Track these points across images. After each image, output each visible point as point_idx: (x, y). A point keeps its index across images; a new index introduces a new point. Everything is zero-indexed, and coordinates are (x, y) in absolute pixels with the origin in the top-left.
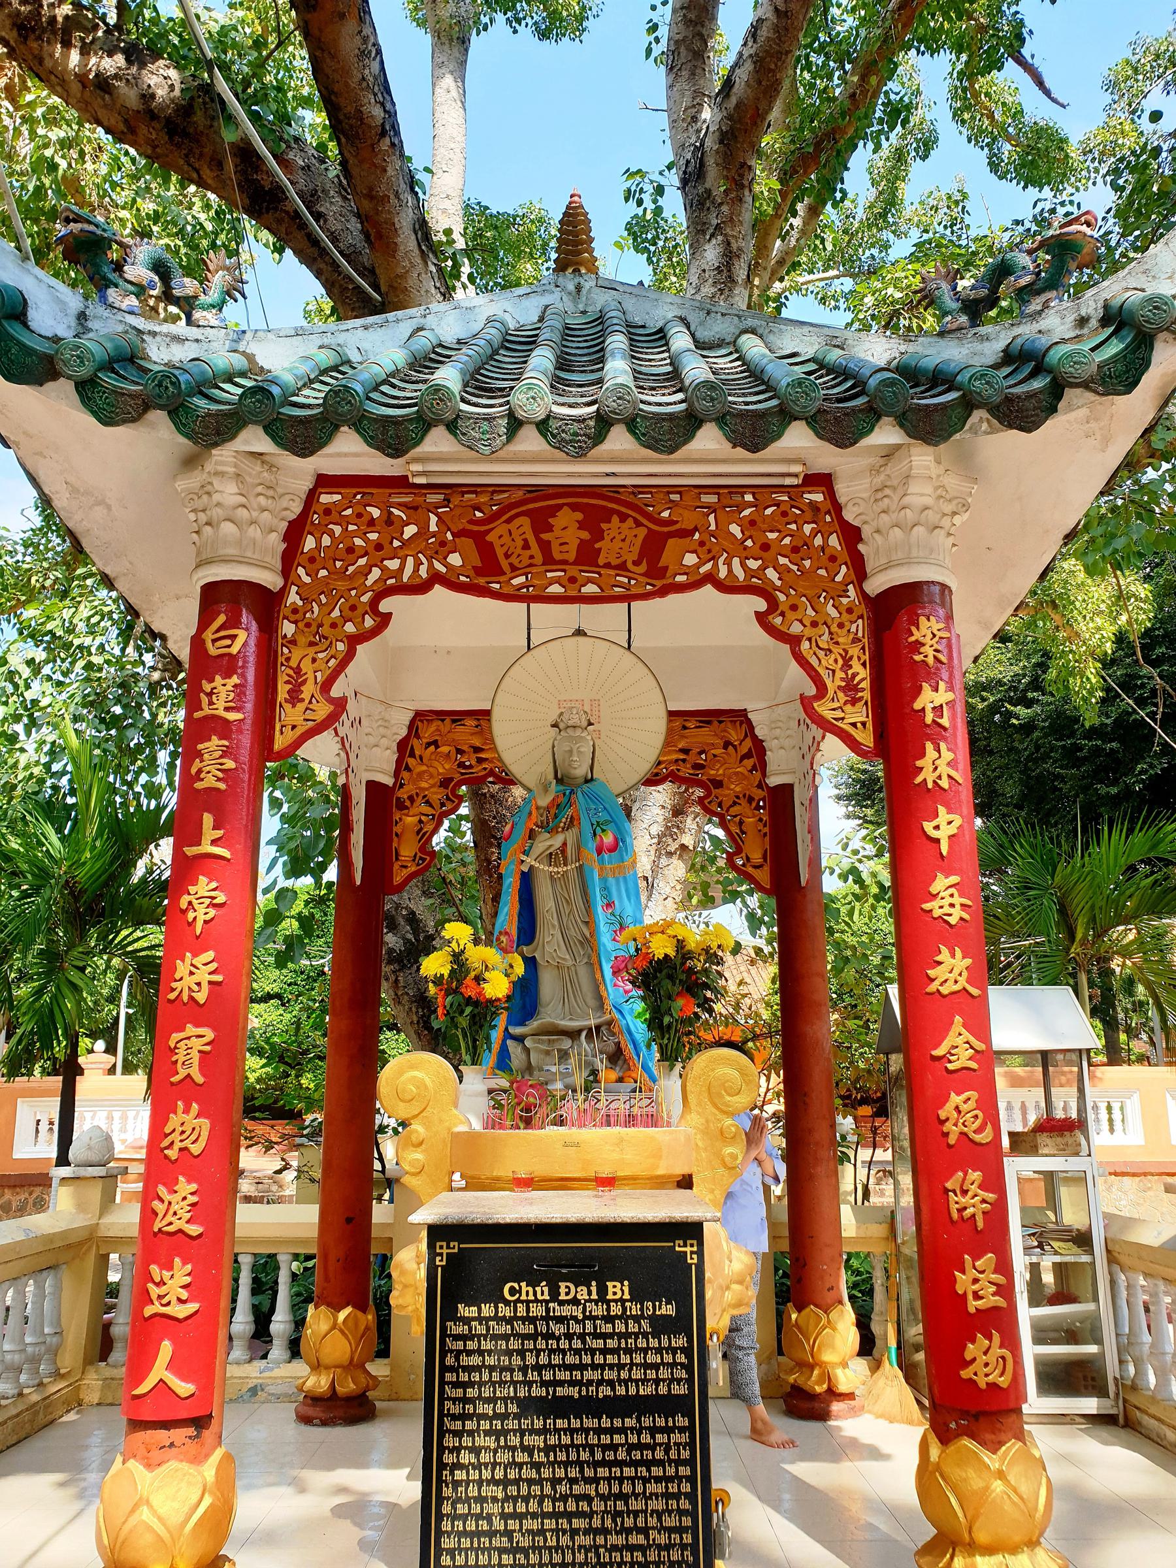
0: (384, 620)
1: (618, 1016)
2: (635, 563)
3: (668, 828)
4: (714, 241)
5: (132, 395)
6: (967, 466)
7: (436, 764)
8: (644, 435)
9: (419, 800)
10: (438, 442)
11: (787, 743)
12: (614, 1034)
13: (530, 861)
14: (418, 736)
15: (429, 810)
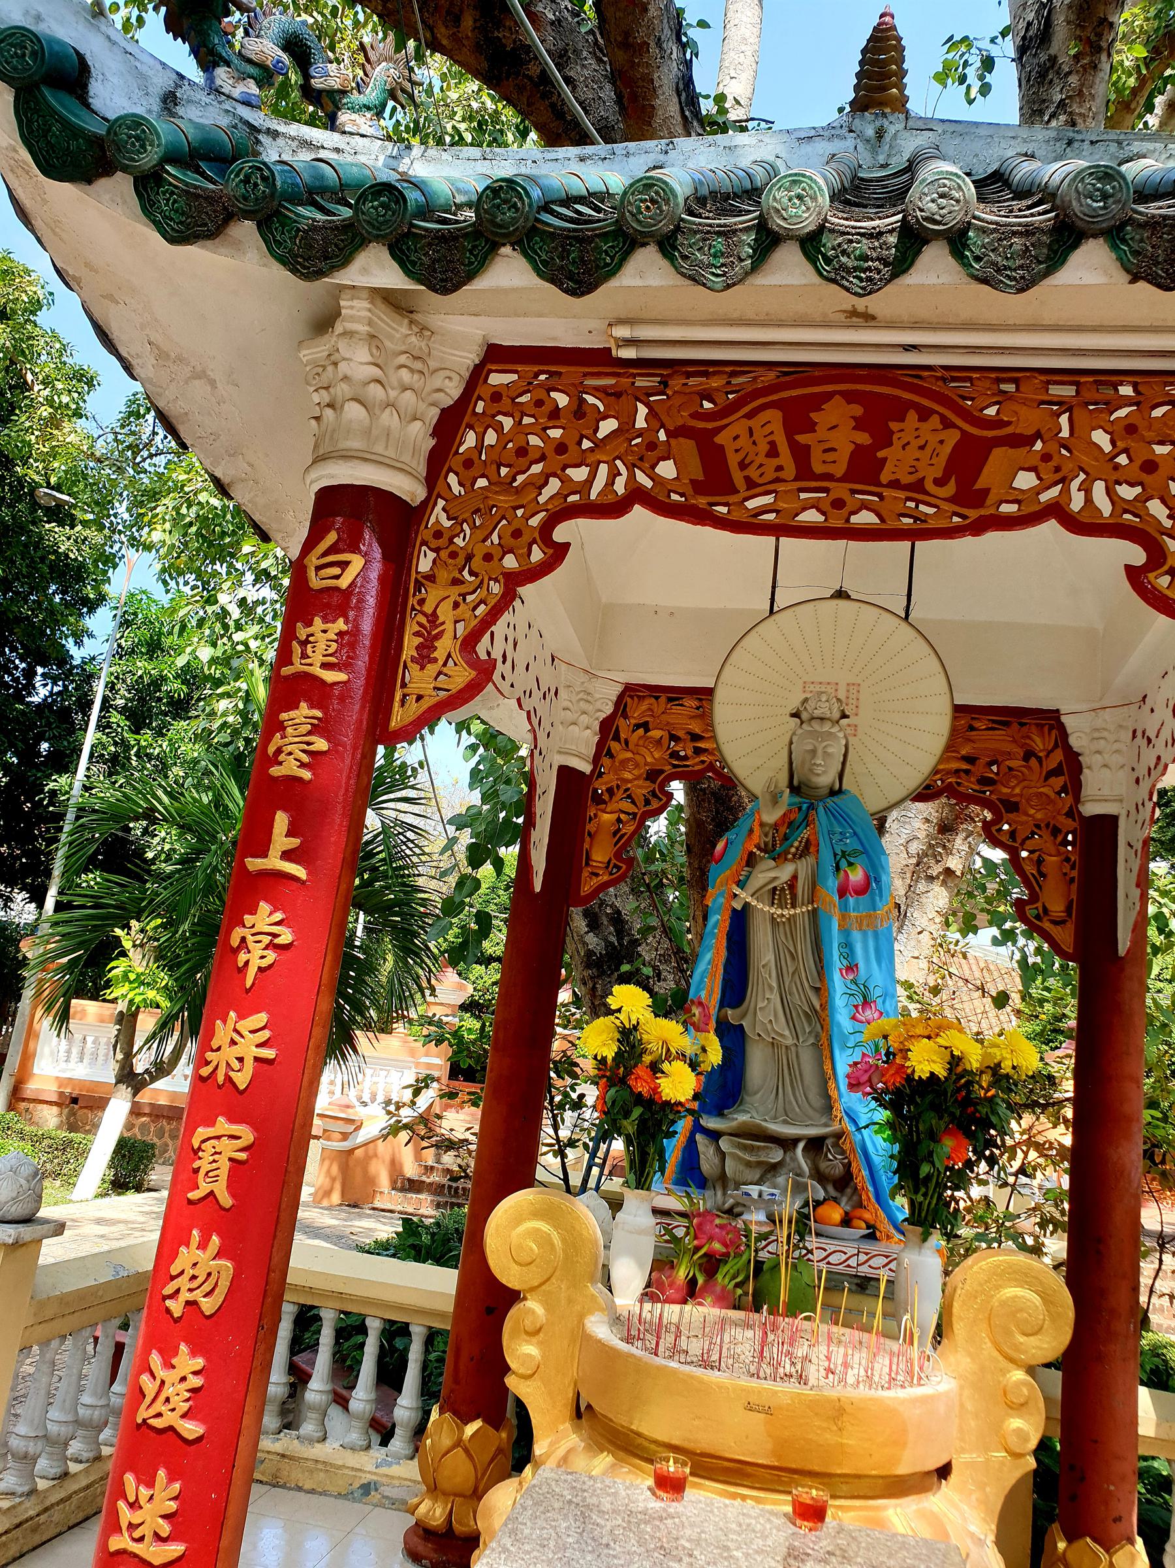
0: (559, 552)
1: (851, 1128)
2: (939, 482)
3: (930, 846)
4: (1054, 123)
7: (643, 751)
8: (978, 259)
9: (620, 794)
10: (645, 274)
12: (843, 1152)
13: (744, 896)
14: (625, 716)
15: (630, 808)
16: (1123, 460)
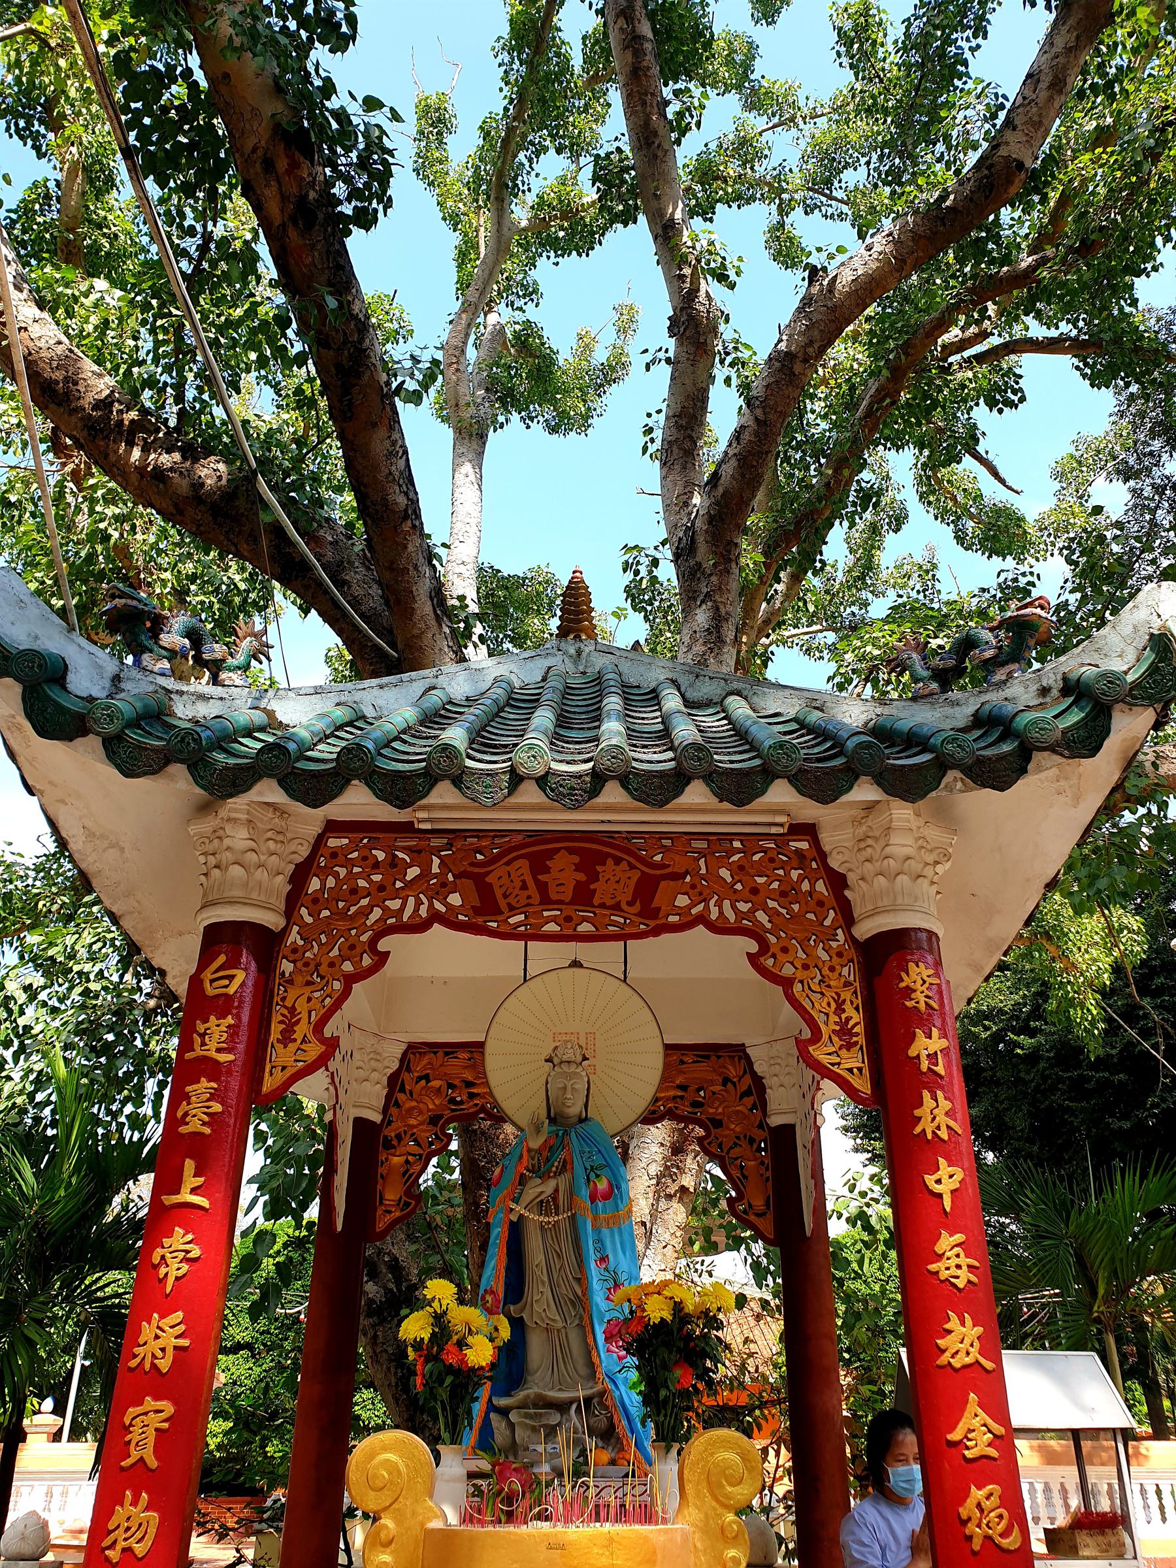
1: (611, 1386)
2: (630, 904)
3: (667, 1168)
5: (156, 750)
6: (946, 818)
10: (443, 794)
11: (787, 1080)
12: (606, 1408)
13: (519, 1209)
14: (409, 1070)
16: (739, 886)
